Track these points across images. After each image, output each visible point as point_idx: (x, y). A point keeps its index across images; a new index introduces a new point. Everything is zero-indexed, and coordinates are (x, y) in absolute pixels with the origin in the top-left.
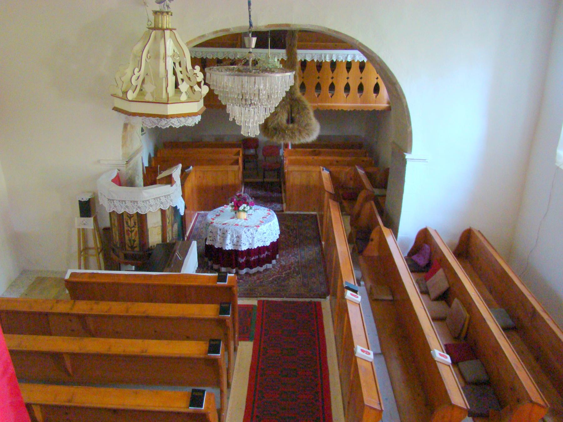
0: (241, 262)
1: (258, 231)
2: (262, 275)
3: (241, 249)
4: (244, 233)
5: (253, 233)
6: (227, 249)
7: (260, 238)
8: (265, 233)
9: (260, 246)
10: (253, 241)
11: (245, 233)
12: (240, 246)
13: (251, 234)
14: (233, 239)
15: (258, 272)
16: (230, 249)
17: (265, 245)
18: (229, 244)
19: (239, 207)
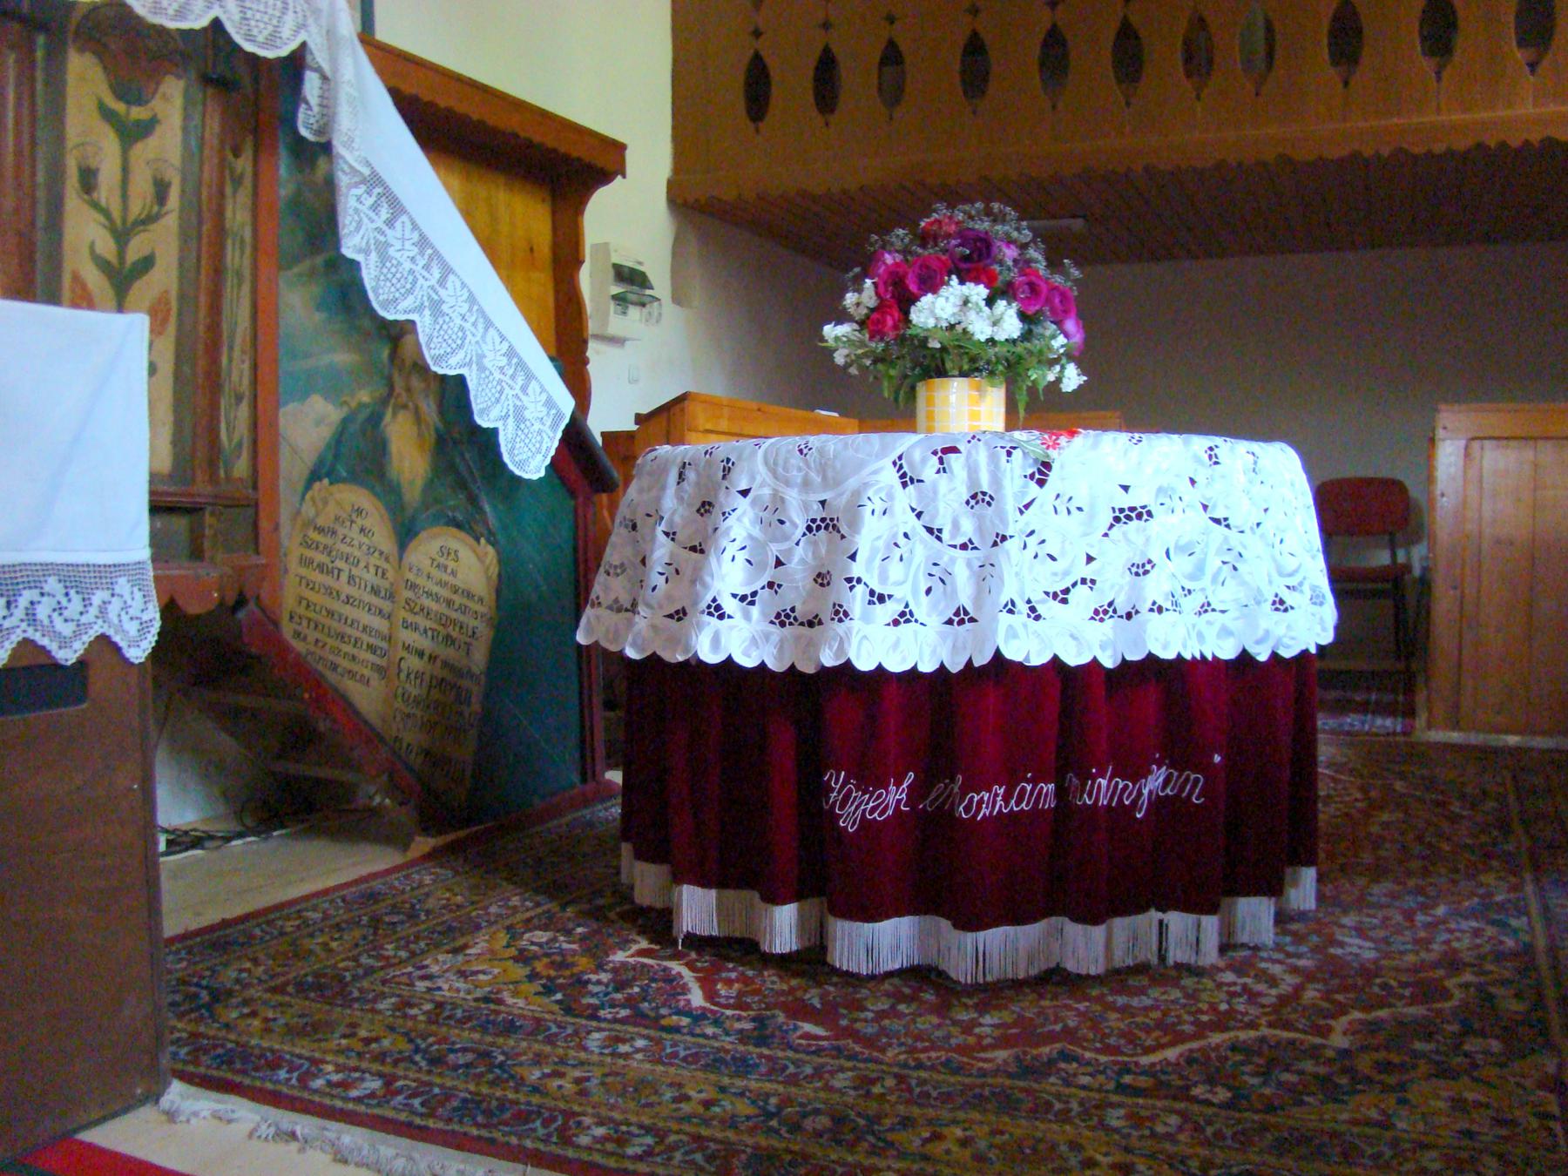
0: (848, 822)
1: (1053, 477)
2: (1071, 1012)
3: (841, 649)
4: (891, 476)
5: (996, 480)
6: (711, 657)
7: (1088, 572)
8: (1139, 514)
9: (1073, 658)
10: (985, 574)
11: (906, 480)
12: (841, 614)
13: (977, 498)
14: (775, 549)
15: (1055, 980)
16: (747, 661)
17: (1135, 656)
18: (730, 606)
19: (906, 301)
